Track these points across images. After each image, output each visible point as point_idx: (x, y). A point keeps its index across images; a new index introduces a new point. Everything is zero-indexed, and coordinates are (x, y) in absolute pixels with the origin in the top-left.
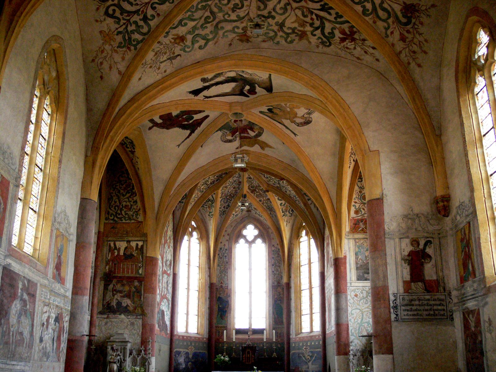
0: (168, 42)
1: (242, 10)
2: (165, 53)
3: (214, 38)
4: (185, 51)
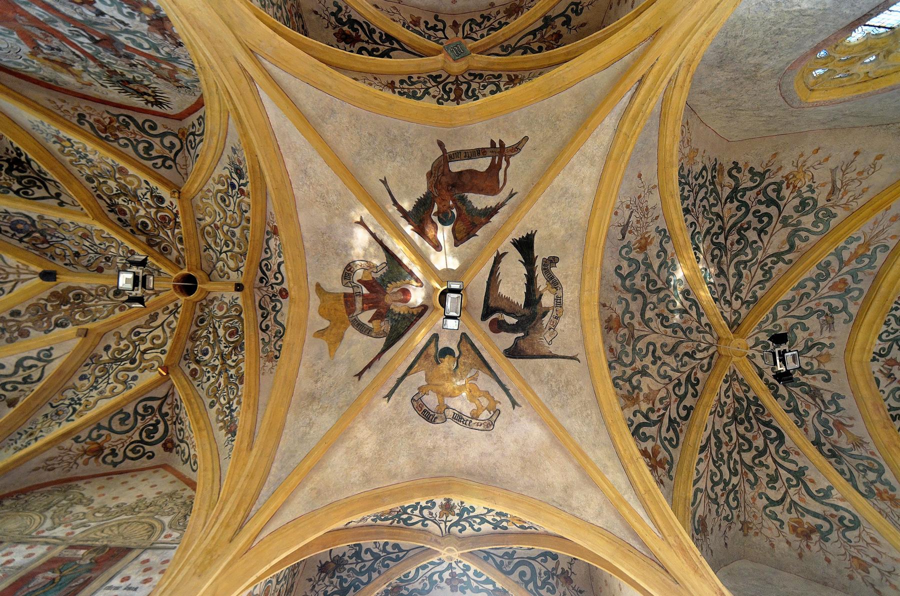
0: (649, 229)
1: (660, 325)
2: (638, 222)
3: (623, 286)
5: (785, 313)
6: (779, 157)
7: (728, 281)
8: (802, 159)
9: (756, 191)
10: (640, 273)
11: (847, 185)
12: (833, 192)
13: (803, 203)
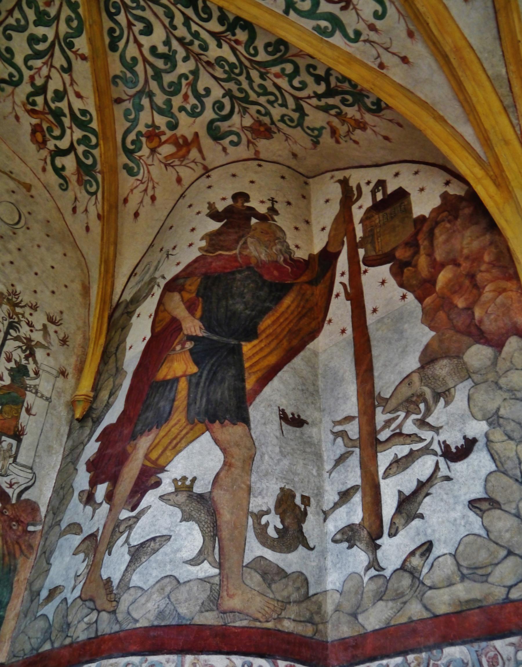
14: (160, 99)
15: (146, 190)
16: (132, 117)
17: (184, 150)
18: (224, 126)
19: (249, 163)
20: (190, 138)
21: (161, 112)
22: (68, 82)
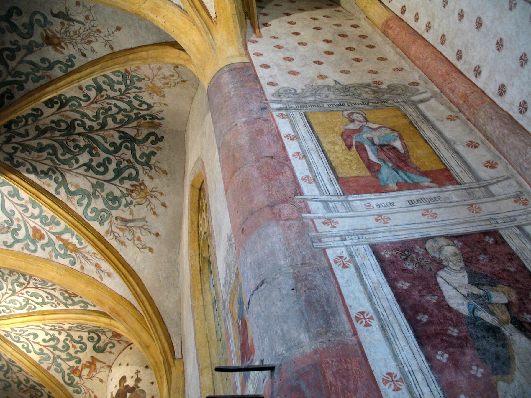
0: (70, 46)
2: (75, 32)
4: (45, 18)
5: (6, 193)
6: (163, 176)
7: (34, 139)
8: (158, 195)
9: (132, 159)
10: (17, 38)
11: (130, 230)
12: (123, 220)
13: (115, 199)
14: (64, 356)
15: (90, 396)
16: (60, 370)
17: (93, 367)
18: (101, 344)
19: (125, 350)
20: (90, 360)
21: (69, 360)
22: (26, 375)
